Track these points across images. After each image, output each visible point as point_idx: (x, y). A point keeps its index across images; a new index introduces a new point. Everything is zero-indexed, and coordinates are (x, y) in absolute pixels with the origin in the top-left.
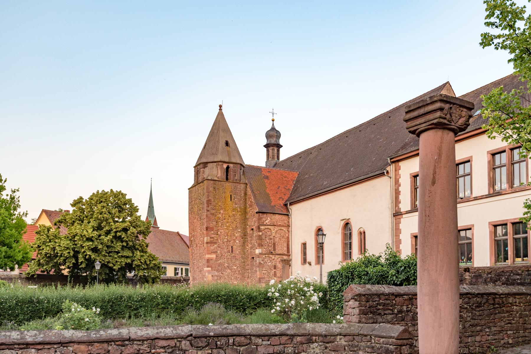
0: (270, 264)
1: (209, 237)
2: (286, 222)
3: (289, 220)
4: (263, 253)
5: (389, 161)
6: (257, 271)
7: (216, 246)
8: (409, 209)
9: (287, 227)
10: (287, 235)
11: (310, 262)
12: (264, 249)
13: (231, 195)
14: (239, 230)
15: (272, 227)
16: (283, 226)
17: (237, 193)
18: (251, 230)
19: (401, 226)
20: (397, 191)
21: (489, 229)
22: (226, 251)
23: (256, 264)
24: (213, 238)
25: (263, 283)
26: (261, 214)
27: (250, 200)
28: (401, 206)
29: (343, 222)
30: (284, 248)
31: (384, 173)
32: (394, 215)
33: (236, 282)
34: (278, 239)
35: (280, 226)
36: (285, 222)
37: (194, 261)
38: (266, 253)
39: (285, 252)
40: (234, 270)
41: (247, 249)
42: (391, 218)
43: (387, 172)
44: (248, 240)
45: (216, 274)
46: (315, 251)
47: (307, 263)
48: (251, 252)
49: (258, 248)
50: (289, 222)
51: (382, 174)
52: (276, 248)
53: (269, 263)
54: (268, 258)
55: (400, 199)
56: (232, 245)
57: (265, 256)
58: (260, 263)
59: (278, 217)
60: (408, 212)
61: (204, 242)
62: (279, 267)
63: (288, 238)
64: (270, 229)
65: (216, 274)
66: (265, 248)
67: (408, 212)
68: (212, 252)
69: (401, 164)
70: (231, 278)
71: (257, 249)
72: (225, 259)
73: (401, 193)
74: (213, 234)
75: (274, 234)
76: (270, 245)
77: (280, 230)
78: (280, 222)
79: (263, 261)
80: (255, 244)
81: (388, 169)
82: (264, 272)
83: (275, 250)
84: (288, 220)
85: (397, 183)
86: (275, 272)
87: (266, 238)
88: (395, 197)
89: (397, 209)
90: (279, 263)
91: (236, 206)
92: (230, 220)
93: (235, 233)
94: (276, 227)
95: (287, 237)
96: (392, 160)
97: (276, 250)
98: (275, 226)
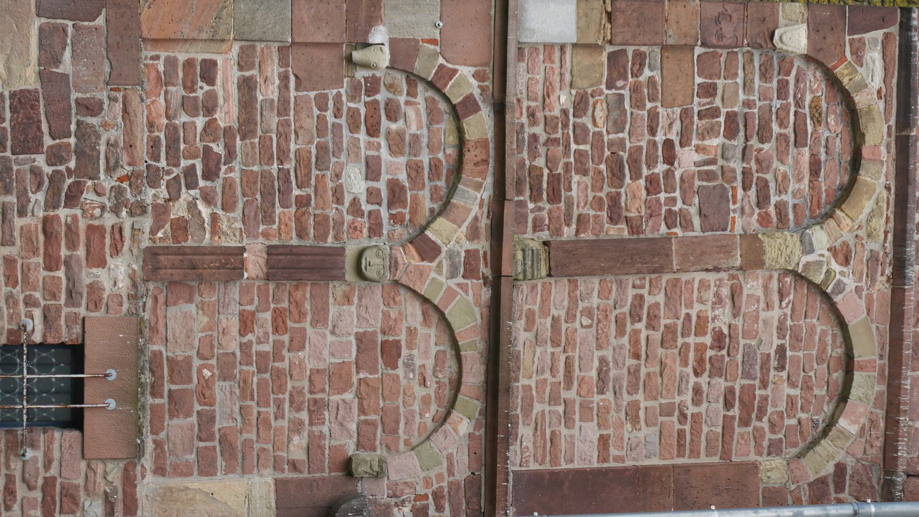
12: (564, 99)
15: (882, 225)
30: (592, 431)
34: (723, 318)
38: (517, 117)
39: (525, 431)
53: (372, 170)
54: (446, 155)
57: (470, 105)
58: (373, 20)
66: (581, 104)
87: (731, 133)
94: (882, 286)
95: (755, 466)
97: (560, 290)
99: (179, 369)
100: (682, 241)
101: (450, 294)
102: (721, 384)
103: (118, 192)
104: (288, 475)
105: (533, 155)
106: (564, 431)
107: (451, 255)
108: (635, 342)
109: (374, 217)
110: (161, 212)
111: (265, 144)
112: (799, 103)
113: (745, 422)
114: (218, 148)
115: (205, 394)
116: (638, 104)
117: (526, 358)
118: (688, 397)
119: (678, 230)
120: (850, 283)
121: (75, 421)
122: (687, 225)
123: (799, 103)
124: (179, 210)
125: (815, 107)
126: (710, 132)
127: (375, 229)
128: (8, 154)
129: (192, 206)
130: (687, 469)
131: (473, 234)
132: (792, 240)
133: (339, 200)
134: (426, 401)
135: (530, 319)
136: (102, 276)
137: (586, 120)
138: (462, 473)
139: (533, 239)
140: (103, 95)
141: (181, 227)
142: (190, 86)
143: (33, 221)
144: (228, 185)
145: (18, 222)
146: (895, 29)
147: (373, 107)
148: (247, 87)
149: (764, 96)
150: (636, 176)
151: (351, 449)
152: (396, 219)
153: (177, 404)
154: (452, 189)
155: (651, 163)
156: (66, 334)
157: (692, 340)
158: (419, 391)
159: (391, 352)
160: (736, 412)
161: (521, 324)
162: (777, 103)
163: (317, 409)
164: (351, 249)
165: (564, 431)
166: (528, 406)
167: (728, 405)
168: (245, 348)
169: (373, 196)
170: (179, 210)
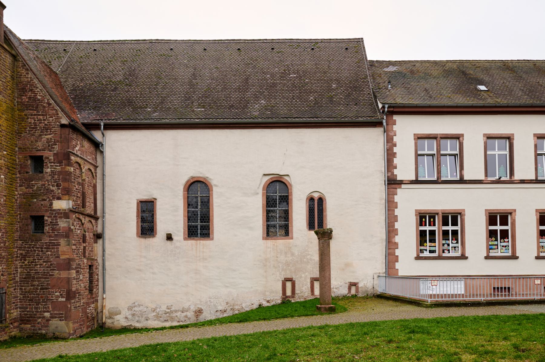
6: (60, 245)
18: (28, 158)
20: (390, 152)
21: (537, 217)
23: (53, 230)
26: (71, 130)
44: (17, 178)
49: (67, 197)
69: (395, 117)
71: (59, 198)
80: (54, 188)
88: (387, 159)
89: (390, 174)
146: (71, 154)
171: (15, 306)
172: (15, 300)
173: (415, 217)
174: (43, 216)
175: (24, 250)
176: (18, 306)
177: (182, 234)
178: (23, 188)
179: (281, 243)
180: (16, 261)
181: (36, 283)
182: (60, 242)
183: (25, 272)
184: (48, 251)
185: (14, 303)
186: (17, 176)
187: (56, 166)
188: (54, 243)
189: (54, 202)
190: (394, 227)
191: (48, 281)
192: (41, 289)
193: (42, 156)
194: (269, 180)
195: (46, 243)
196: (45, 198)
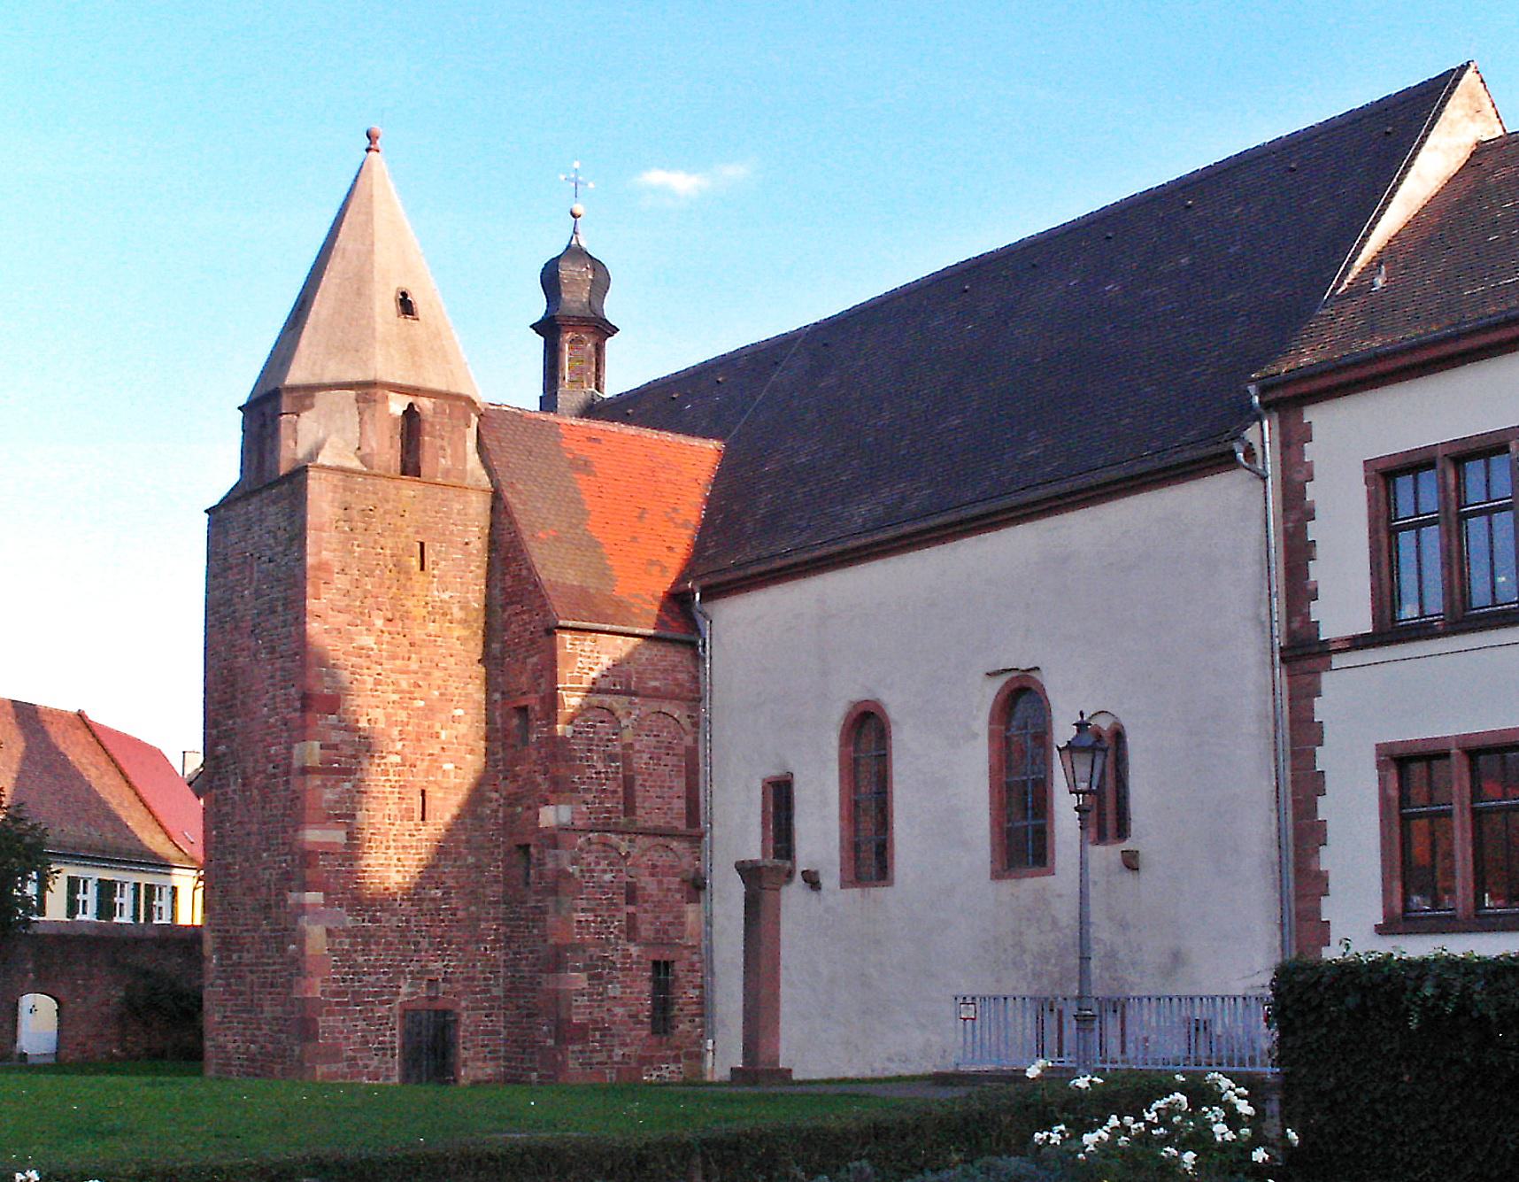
0: (608, 877)
1: (317, 744)
2: (682, 677)
3: (696, 667)
4: (579, 824)
5: (1256, 399)
6: (546, 913)
7: (348, 785)
8: (1363, 624)
9: (682, 699)
10: (688, 740)
11: (816, 873)
12: (584, 808)
13: (422, 544)
14: (459, 712)
16: (672, 697)
17: (452, 533)
19: (1322, 709)
22: (393, 809)
24: (335, 747)
25: (575, 969)
27: (513, 567)
28: (1317, 611)
29: (999, 682)
30: (676, 800)
31: (1233, 453)
32: (1287, 654)
33: (439, 965)
34: (646, 756)
35: (656, 694)
36: (680, 676)
37: (230, 859)
39: (675, 823)
40: (432, 906)
41: (494, 805)
42: (1269, 671)
43: (1250, 453)
45: (349, 921)
46: (842, 818)
47: (798, 877)
48: (511, 819)
50: (695, 679)
51: (1225, 462)
52: (638, 801)
53: (604, 871)
55: (1312, 579)
56: (425, 784)
59: (648, 652)
60: (1358, 643)
61: (290, 765)
62: (651, 895)
63: (691, 756)
64: (611, 712)
65: (349, 921)
67: (1358, 643)
68: (329, 817)
70: (417, 944)
72: (391, 851)
73: (1320, 551)
74: (334, 727)
75: (628, 736)
76: (610, 785)
77: (654, 717)
78: (656, 679)
79: (574, 862)
80: (539, 778)
81: (1251, 434)
82: (582, 916)
83: (630, 809)
84: (692, 670)
85: (1296, 509)
86: (631, 917)
89: (1295, 625)
90: (652, 875)
91: (445, 596)
92: (414, 666)
93: (437, 728)
94: (637, 700)
96: (1270, 396)
97: (640, 812)
98: (635, 694)
99: (658, 931)
100: (624, 770)
101: (640, 848)
102: (664, 757)
103: (613, 950)
104: (685, 899)
105: (599, 819)
106: (675, 811)
107: (629, 847)
108: (651, 787)
109: (617, 871)
110: (617, 937)
111: (598, 905)
112: (582, 726)
113: (673, 749)
114: (599, 919)
115: (665, 923)
116: (584, 783)
117: (656, 823)
118: (667, 769)
119: (621, 770)
120: (637, 712)
121: (666, 963)
122: (618, 767)
123: (582, 726)
124: (616, 932)
125: (585, 721)
126: (592, 758)
127: (621, 871)
128: (603, 982)
129: (615, 928)
130: (687, 771)
131: (623, 840)
132: (625, 732)
133: (612, 882)
134: (667, 856)
135: (646, 821)
136: (635, 955)
137: (590, 801)
138: (686, 845)
139: (623, 820)
140: (588, 954)
141: (621, 931)
142: (583, 928)
143: (620, 975)
144: (609, 916)
145: (621, 979)
146: (564, 693)
147: (589, 871)
148: (583, 910)
149: (581, 739)
150: (604, 784)
151: (678, 879)
152: (618, 863)
153: (666, 932)
154: (611, 846)
155: (601, 779)
156: (650, 964)
157: (652, 767)
158: (665, 858)
159: (654, 866)
160: (671, 752)
161: (647, 825)
162: (584, 735)
163: (669, 890)
164: (629, 880)
165: (675, 811)
166: (668, 823)
167: (668, 754)
168: (652, 911)
169: (612, 871)
170: (616, 932)
171: (489, 1052)
172: (489, 1040)
173: (1374, 774)
174: (528, 846)
175: (508, 926)
176: (501, 1054)
177: (837, 870)
178: (508, 781)
179: (1029, 886)
180: (493, 949)
181: (521, 1002)
182: (547, 906)
183: (508, 977)
184: (533, 927)
185: (487, 1046)
186: (499, 756)
187: (544, 726)
188: (540, 907)
189: (540, 810)
190: (1316, 817)
191: (534, 998)
192: (528, 1016)
193: (527, 706)
194: (1002, 689)
195: (531, 907)
196: (530, 802)
